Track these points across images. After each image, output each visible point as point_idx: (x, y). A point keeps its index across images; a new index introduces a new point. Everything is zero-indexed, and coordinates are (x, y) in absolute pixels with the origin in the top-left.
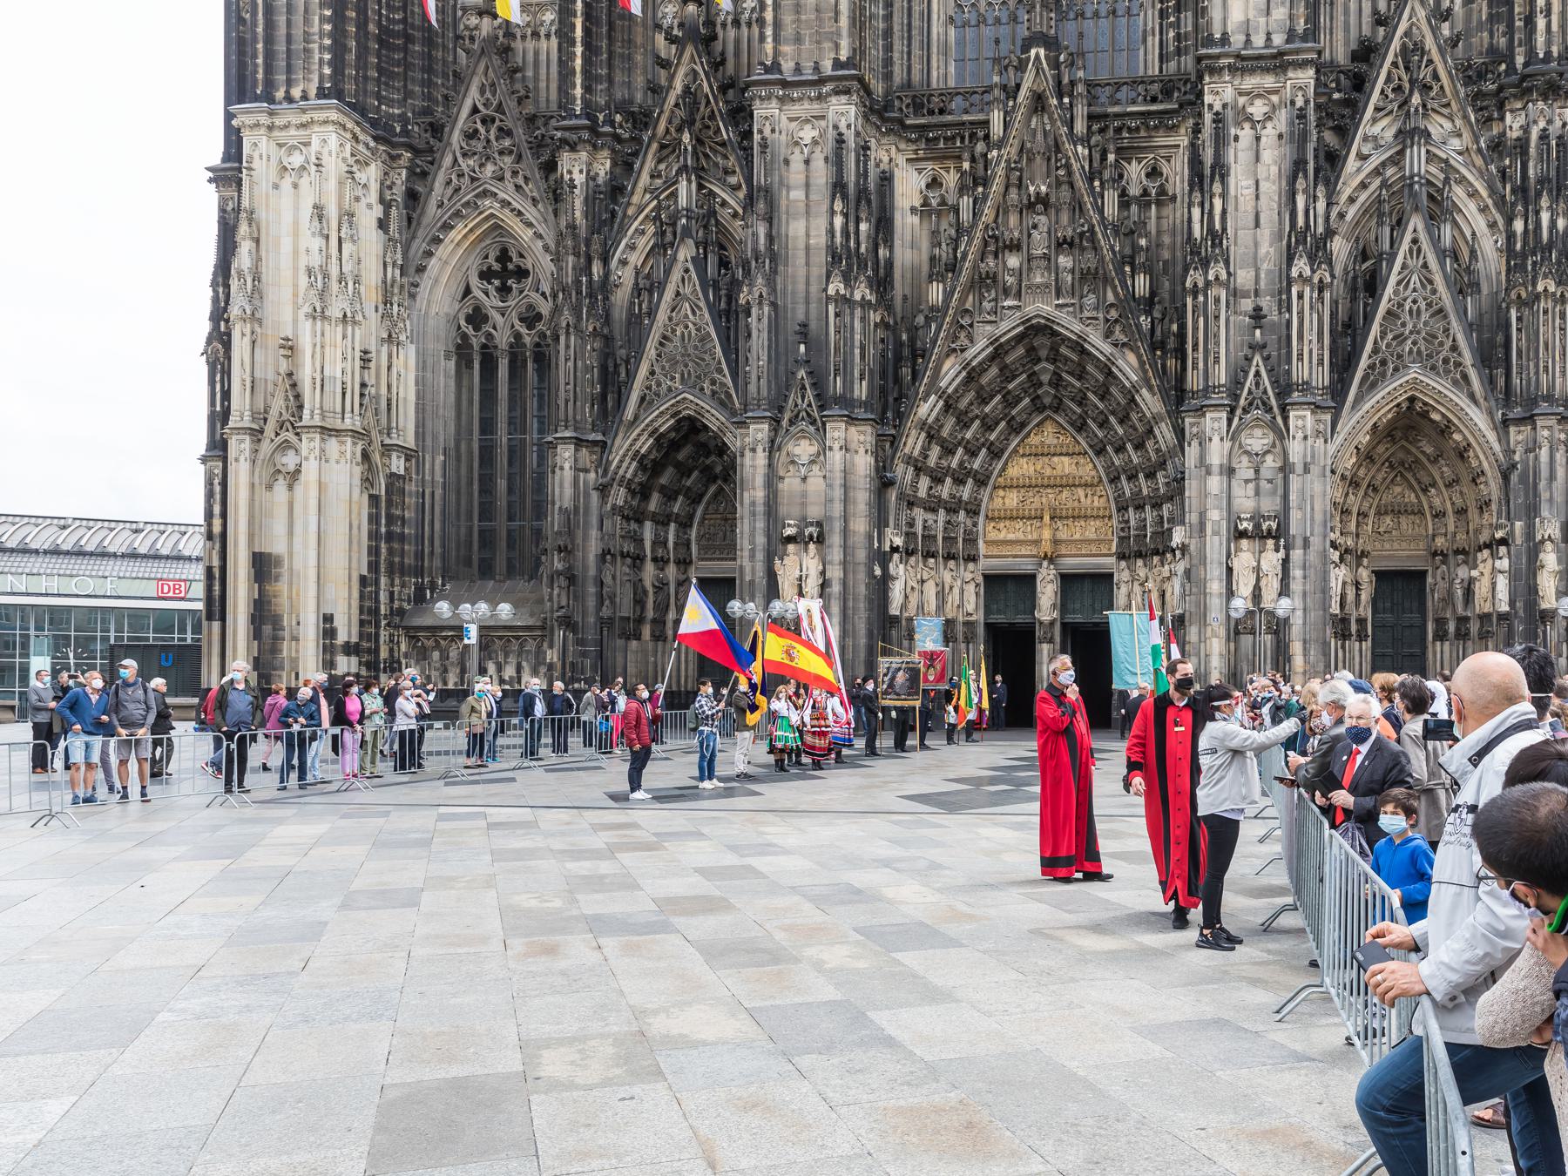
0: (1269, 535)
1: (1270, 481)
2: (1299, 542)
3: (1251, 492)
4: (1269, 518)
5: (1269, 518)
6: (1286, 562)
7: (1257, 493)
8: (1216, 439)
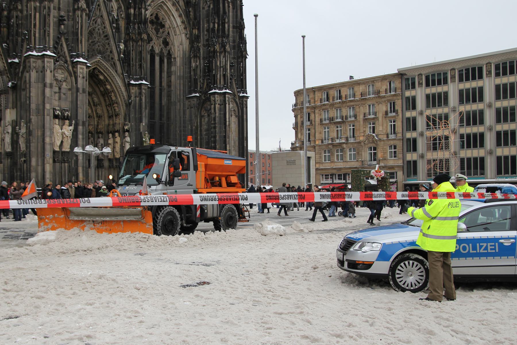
0: (68, 118)
1: (64, 94)
2: (81, 123)
3: (57, 98)
4: (67, 111)
5: (67, 111)
6: (75, 131)
7: (60, 99)
8: (48, 71)
